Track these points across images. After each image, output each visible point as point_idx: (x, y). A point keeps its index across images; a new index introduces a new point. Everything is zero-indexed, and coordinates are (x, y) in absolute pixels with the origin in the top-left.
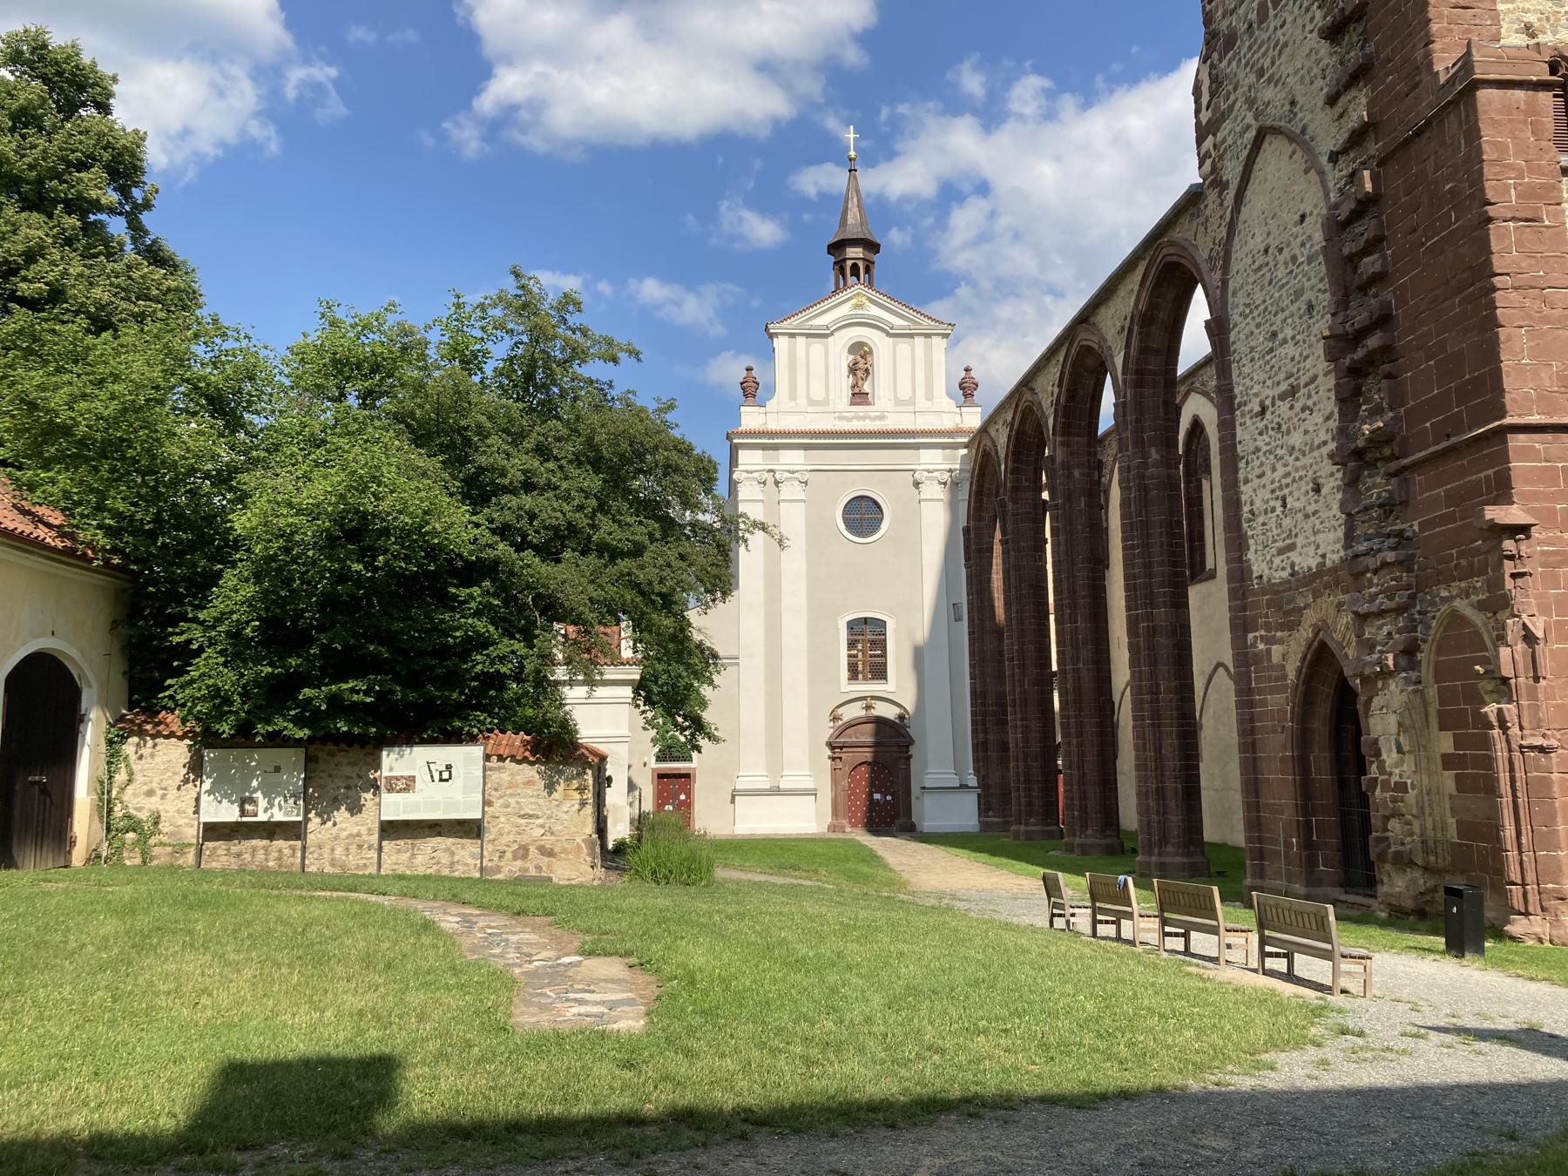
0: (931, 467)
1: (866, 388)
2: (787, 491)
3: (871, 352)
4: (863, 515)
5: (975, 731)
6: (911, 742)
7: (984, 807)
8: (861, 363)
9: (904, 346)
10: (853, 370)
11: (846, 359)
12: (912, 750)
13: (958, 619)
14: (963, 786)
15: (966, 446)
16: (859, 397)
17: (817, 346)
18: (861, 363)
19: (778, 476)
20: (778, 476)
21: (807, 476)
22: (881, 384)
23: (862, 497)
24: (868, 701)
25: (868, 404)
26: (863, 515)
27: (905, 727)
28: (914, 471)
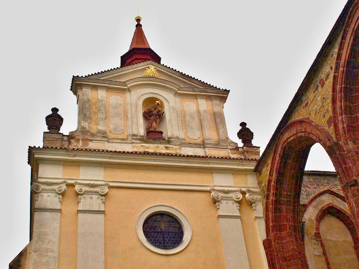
0: (226, 189)
2: (86, 203)
3: (161, 105)
8: (153, 113)
10: (147, 115)
16: (153, 135)
18: (153, 113)
19: (77, 188)
20: (77, 188)
21: (106, 190)
22: (170, 128)
26: (163, 230)
28: (210, 192)
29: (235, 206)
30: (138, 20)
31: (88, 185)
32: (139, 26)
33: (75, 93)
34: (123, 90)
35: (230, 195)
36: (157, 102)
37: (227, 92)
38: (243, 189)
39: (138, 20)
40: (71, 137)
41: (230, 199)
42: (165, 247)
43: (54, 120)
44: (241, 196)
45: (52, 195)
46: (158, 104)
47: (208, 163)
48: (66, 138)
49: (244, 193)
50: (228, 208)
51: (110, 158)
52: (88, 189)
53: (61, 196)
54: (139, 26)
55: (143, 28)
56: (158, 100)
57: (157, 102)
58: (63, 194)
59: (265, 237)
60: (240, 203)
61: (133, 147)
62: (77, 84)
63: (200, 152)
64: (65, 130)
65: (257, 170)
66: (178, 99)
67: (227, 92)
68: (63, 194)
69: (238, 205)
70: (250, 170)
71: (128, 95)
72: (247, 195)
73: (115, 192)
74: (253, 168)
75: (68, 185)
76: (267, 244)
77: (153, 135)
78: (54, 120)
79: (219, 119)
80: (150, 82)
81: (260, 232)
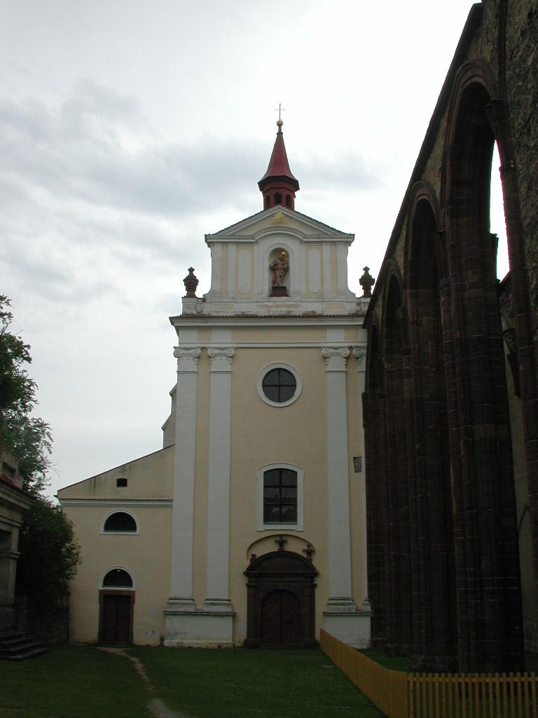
0: (336, 345)
1: (284, 285)
2: (217, 364)
3: (287, 256)
4: (279, 384)
5: (369, 565)
6: (314, 574)
7: (376, 628)
8: (280, 265)
9: (314, 253)
10: (273, 269)
11: (266, 262)
12: (317, 581)
13: (358, 470)
14: (359, 614)
15: (364, 326)
16: (278, 290)
17: (245, 254)
18: (280, 265)
19: (209, 352)
20: (209, 352)
21: (233, 352)
22: (295, 281)
23: (279, 370)
24: (281, 540)
25: (286, 295)
27: (311, 560)
29: (343, 361)
30: (280, 124)
31: (218, 348)
32: (280, 134)
33: (209, 246)
34: (250, 243)
35: (339, 351)
36: (283, 253)
37: (352, 237)
38: (353, 345)
39: (280, 124)
40: (204, 300)
41: (339, 354)
42: (279, 401)
43: (191, 282)
44: (348, 352)
45: (190, 358)
46: (284, 255)
47: (322, 321)
48: (200, 301)
49: (351, 348)
50: (337, 364)
51: (236, 322)
52: (218, 351)
53: (197, 359)
54: (280, 134)
55: (283, 135)
56: (284, 250)
57: (283, 253)
58: (198, 358)
59: (364, 391)
60: (347, 358)
61: (258, 306)
62: (210, 240)
63: (318, 308)
64: (199, 293)
65: (364, 326)
66: (303, 247)
67: (352, 237)
68: (198, 358)
69: (345, 360)
70: (360, 325)
71: (256, 247)
72: (354, 351)
73: (240, 352)
74: (362, 323)
75: (203, 348)
76: (365, 396)
77: (278, 290)
78: (191, 282)
79: (340, 268)
80: (279, 230)
81: (360, 387)
